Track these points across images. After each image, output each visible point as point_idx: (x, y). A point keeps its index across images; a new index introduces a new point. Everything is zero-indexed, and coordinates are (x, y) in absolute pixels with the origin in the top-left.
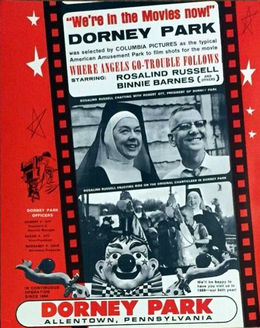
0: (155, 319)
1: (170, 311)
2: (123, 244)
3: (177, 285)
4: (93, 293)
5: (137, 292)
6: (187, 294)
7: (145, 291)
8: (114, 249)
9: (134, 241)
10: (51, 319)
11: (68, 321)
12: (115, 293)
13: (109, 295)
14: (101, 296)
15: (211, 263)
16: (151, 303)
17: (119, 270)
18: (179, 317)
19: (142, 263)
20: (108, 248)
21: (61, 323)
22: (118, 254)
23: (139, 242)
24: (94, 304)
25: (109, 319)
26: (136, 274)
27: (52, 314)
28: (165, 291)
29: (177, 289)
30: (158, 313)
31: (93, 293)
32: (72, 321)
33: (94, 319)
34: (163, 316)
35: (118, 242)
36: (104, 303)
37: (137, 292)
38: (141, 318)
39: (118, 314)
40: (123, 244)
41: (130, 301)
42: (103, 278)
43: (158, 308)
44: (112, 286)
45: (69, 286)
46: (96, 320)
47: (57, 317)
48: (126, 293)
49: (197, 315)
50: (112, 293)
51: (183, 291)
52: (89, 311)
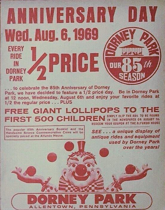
0: (99, 207)
1: (109, 202)
2: (79, 158)
3: (113, 185)
4: (60, 189)
5: (88, 189)
6: (120, 191)
7: (93, 188)
8: (75, 161)
9: (86, 156)
10: (33, 205)
11: (44, 207)
12: (74, 190)
13: (70, 191)
14: (65, 191)
15: (135, 170)
16: (96, 196)
17: (76, 175)
18: (114, 206)
19: (91, 170)
20: (70, 159)
21: (39, 208)
23: (89, 156)
24: (60, 196)
25: (70, 206)
26: (87, 177)
27: (34, 202)
28: (105, 188)
29: (113, 187)
30: (101, 203)
31: (60, 189)
32: (47, 207)
33: (60, 206)
34: (104, 205)
35: (75, 156)
36: (67, 196)
37: (88, 189)
38: (90, 206)
39: (75, 203)
40: (79, 158)
41: (83, 195)
42: (67, 180)
43: (101, 200)
44: (72, 185)
45: (45, 185)
46: (61, 206)
47: (37, 204)
48: (81, 190)
49: (126, 204)
50: (72, 189)
51: (117, 189)
52: (57, 201)
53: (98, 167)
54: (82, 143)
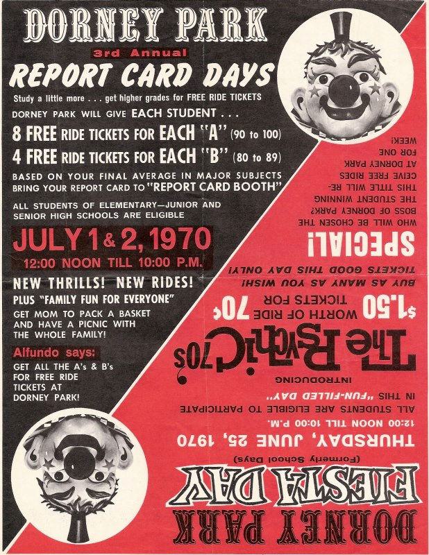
19: (52, 463)
22: (96, 481)
26: (65, 443)
42: (120, 439)
53: (34, 471)
54: (78, 539)
